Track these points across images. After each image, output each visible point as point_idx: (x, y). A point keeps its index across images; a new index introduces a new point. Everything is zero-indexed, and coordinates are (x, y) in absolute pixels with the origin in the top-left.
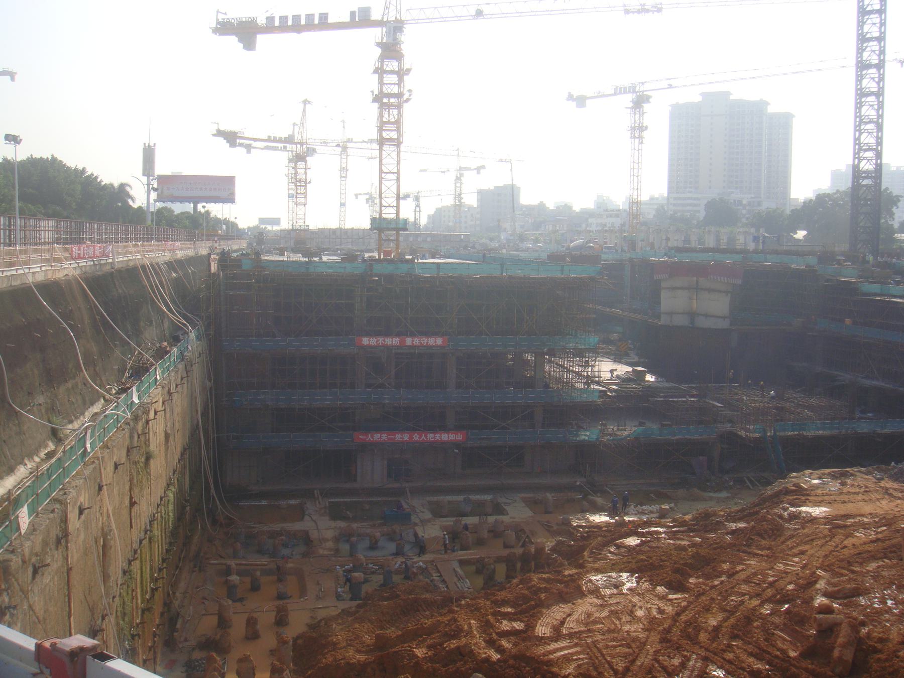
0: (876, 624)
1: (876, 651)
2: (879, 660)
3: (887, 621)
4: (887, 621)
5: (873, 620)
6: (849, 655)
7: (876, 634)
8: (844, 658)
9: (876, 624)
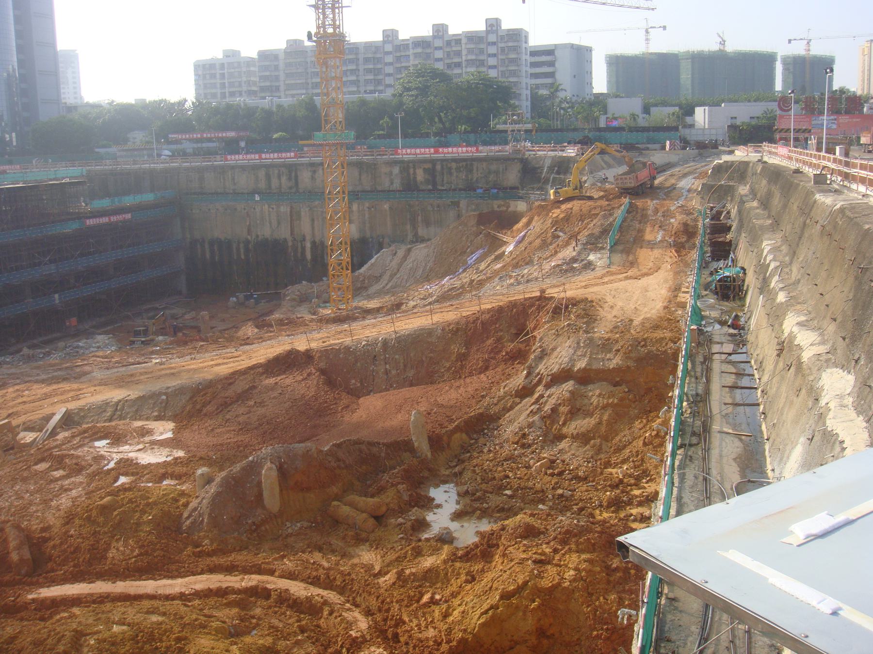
0: (28, 518)
1: (46, 540)
2: (54, 547)
3: (37, 511)
4: (37, 511)
5: (24, 516)
6: (27, 555)
7: (35, 527)
8: (25, 558)
9: (28, 518)
